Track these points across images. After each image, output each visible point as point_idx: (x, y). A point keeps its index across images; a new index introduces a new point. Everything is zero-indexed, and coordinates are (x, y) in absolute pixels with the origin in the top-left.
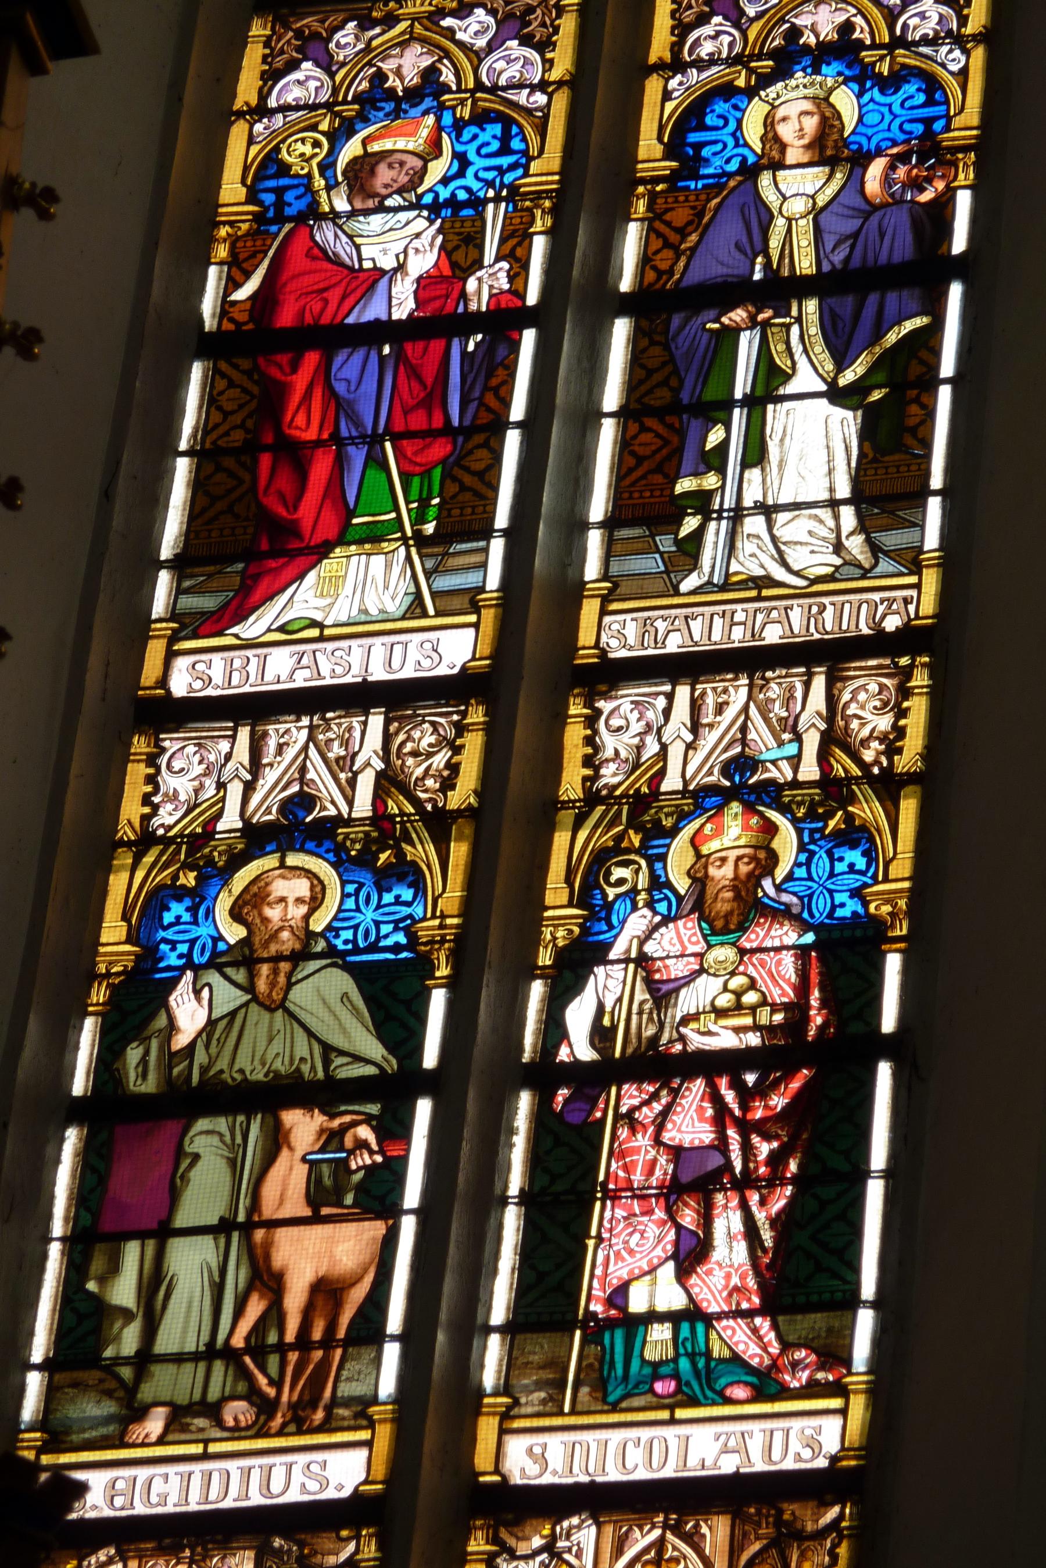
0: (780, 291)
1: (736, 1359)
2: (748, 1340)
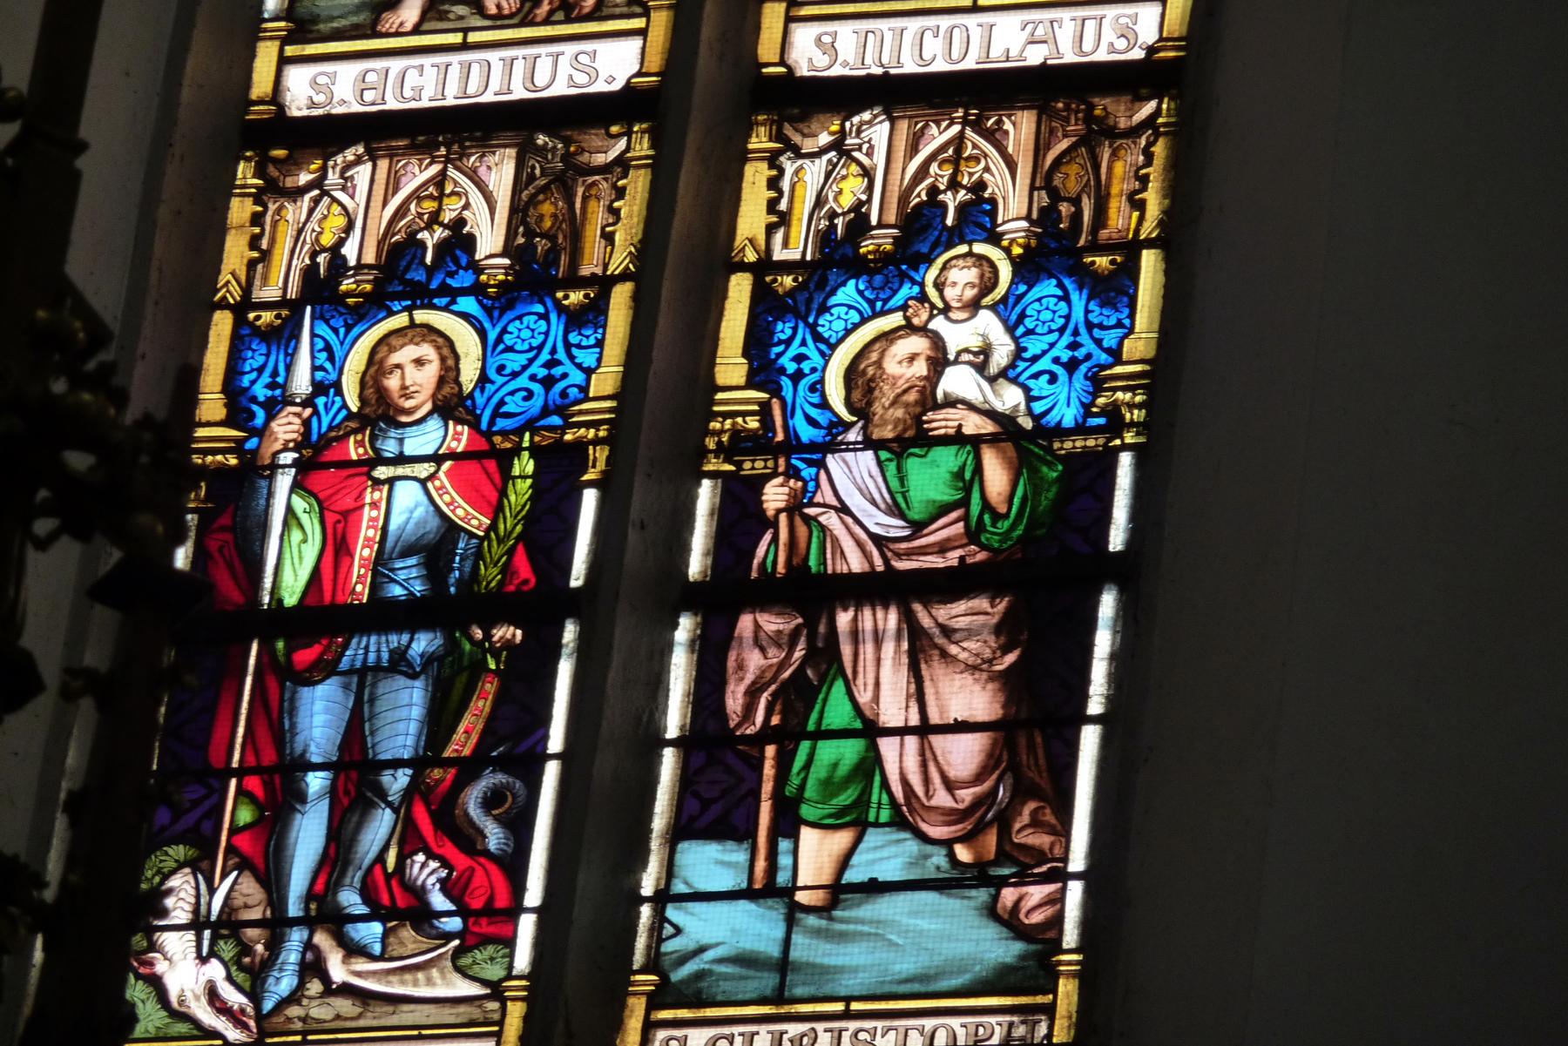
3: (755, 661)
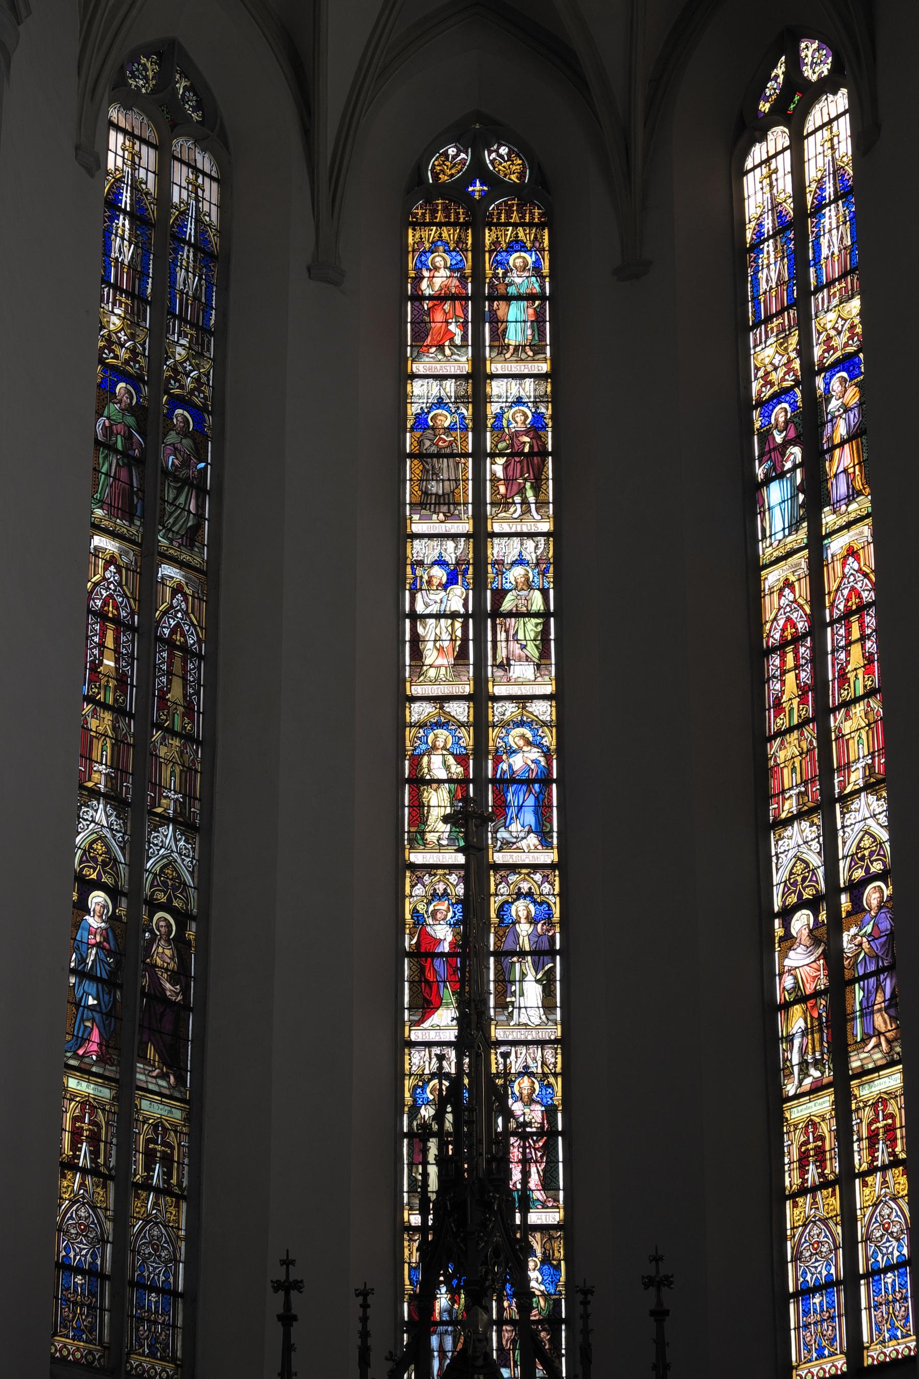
0: (522, 954)
1: (538, 1200)
3: (506, 1335)
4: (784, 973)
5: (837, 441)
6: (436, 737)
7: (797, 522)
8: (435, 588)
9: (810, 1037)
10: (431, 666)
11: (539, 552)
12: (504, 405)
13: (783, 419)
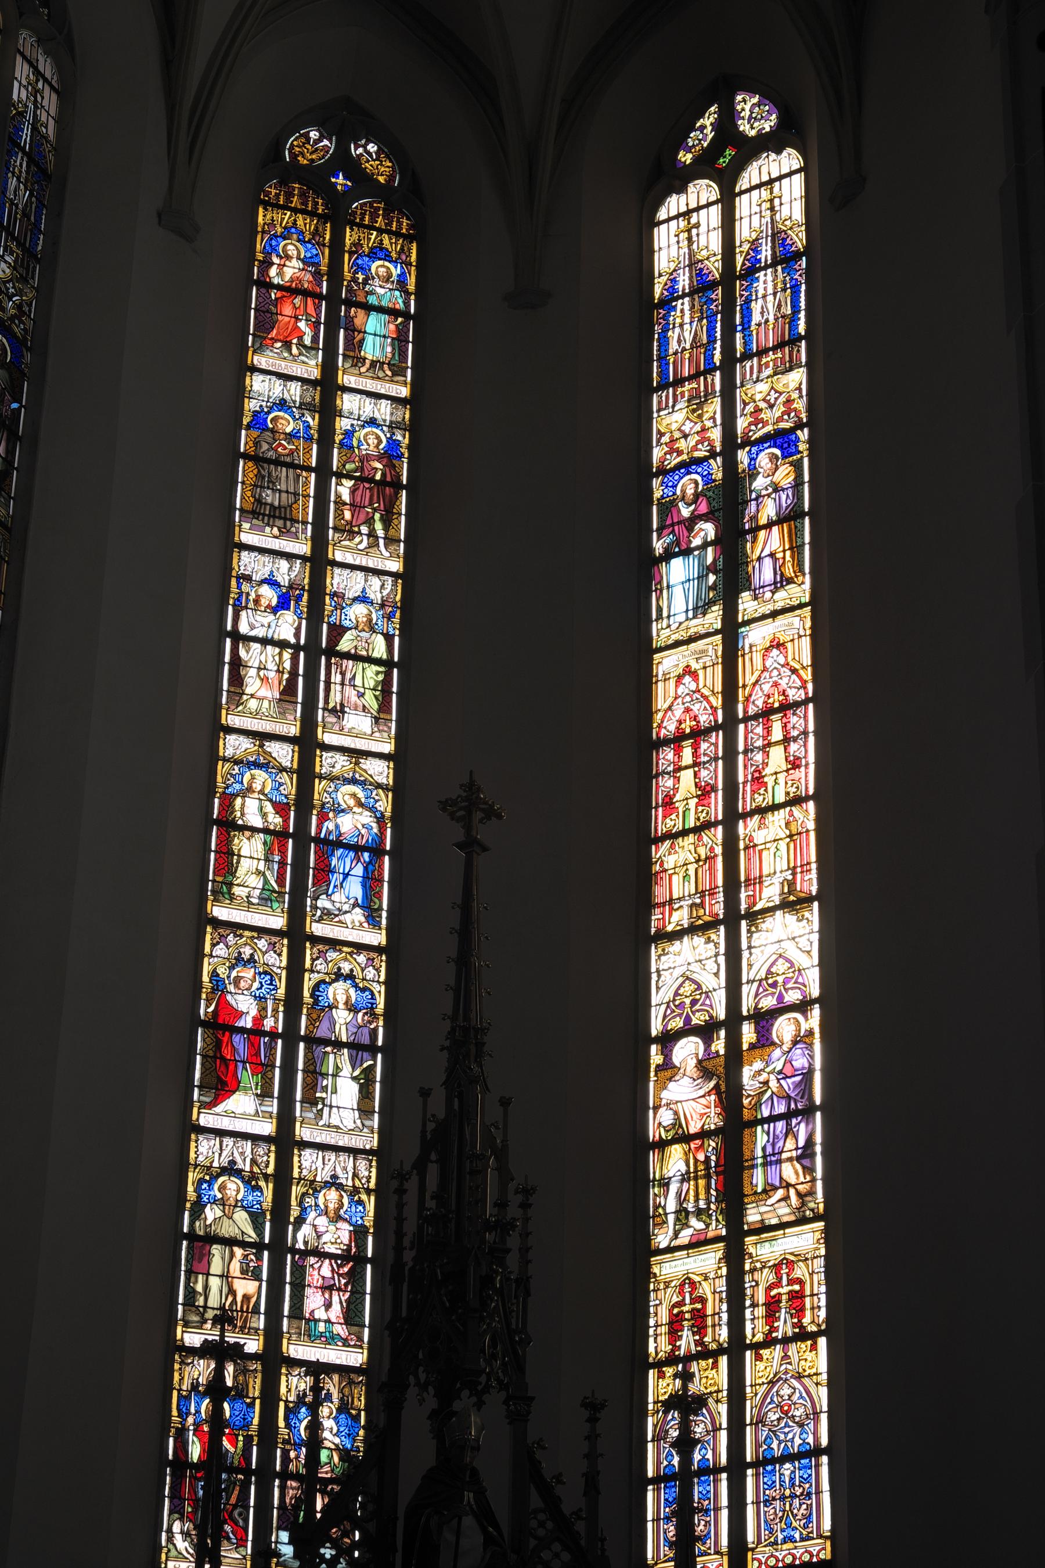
0: (338, 1045)
2: (340, 1330)
3: (291, 1491)
4: (660, 1106)
5: (763, 521)
6: (253, 777)
7: (704, 606)
8: (263, 609)
9: (692, 1183)
10: (252, 696)
11: (385, 593)
12: (355, 422)
13: (692, 491)
